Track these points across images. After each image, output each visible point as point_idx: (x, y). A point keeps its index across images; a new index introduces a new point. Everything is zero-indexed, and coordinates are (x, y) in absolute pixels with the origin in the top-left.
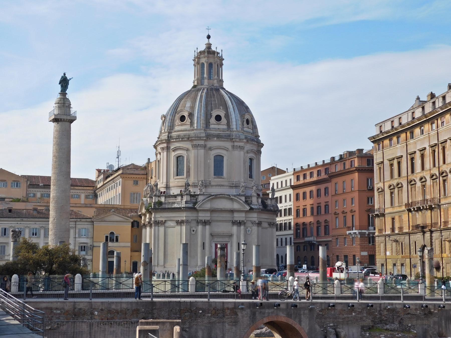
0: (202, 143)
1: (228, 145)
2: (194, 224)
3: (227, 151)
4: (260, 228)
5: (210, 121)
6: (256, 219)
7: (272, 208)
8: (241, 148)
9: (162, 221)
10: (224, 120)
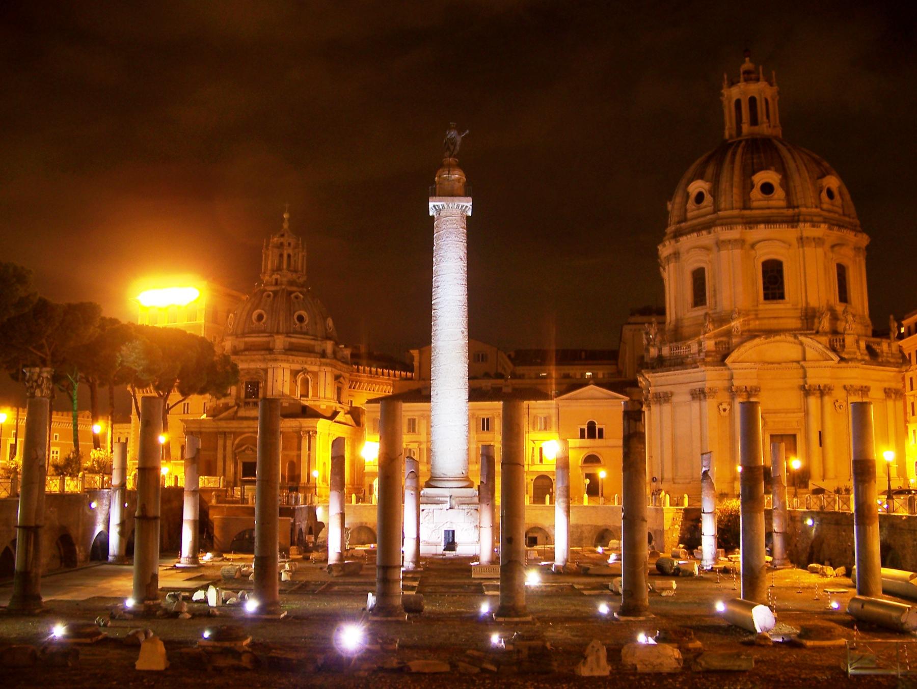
2: (724, 397)
7: (892, 360)
8: (819, 242)
9: (666, 393)
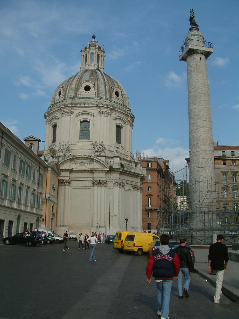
0: (69, 109)
1: (95, 111)
3: (93, 116)
5: (79, 91)
6: (118, 180)
10: (93, 91)
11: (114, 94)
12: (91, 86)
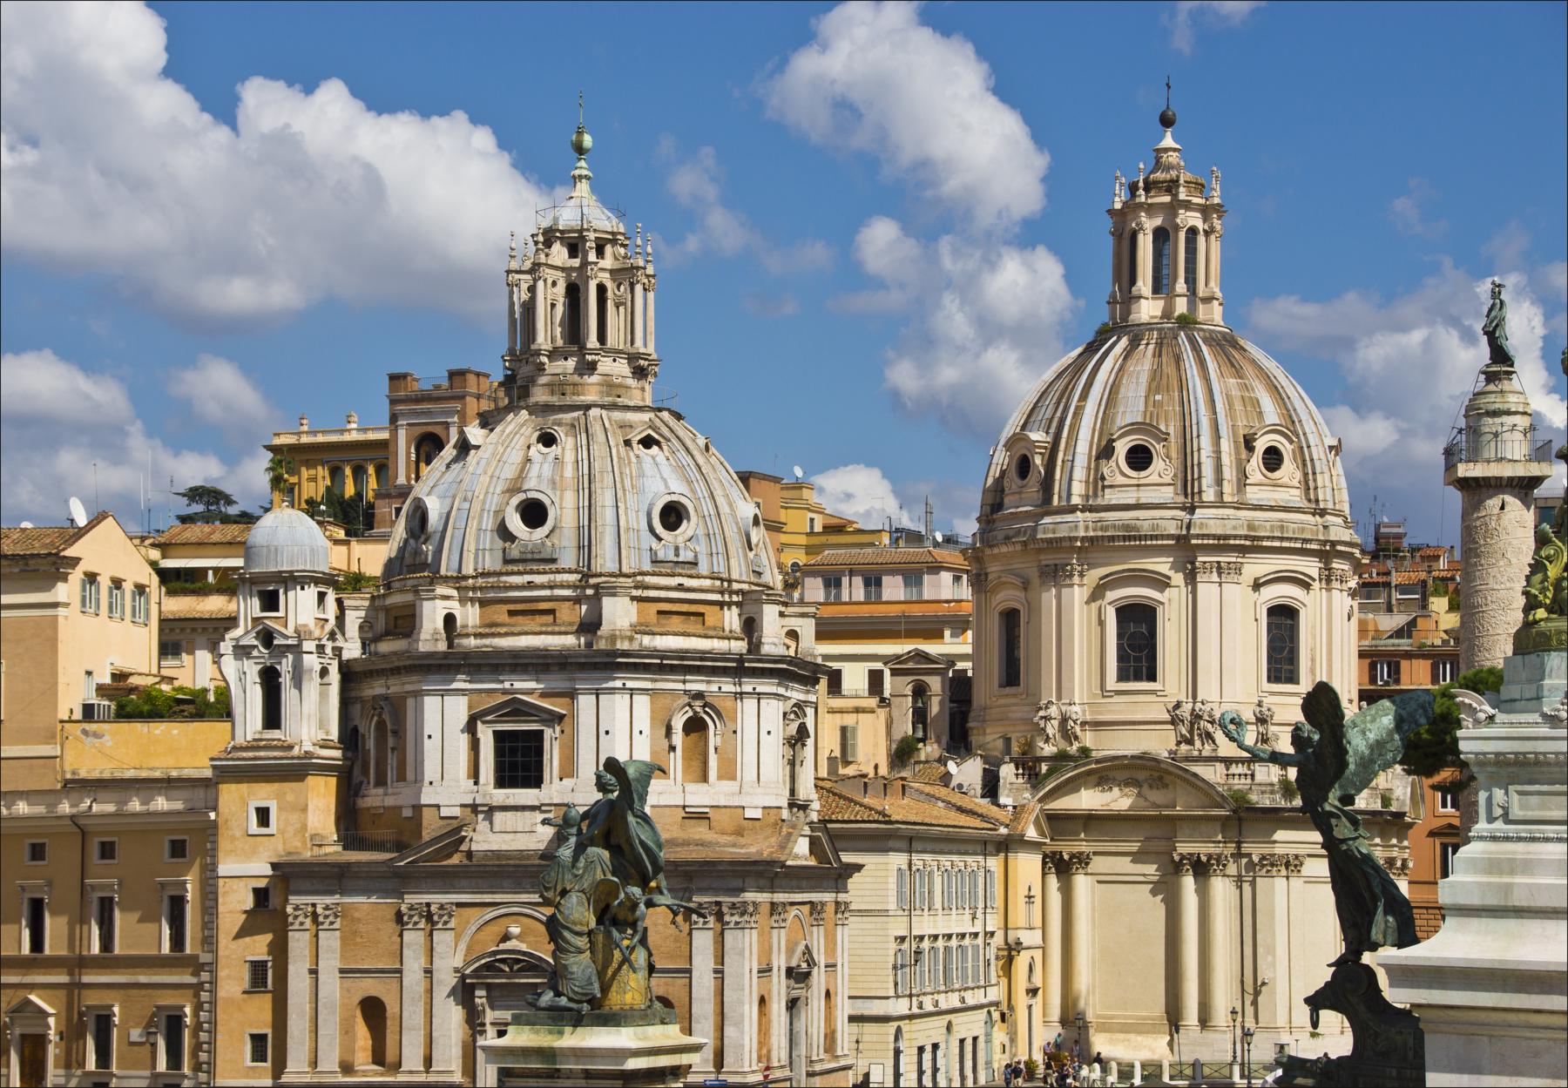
4: (1296, 882)
5: (1106, 471)
10: (1161, 467)
11: (1255, 465)
12: (1157, 448)
